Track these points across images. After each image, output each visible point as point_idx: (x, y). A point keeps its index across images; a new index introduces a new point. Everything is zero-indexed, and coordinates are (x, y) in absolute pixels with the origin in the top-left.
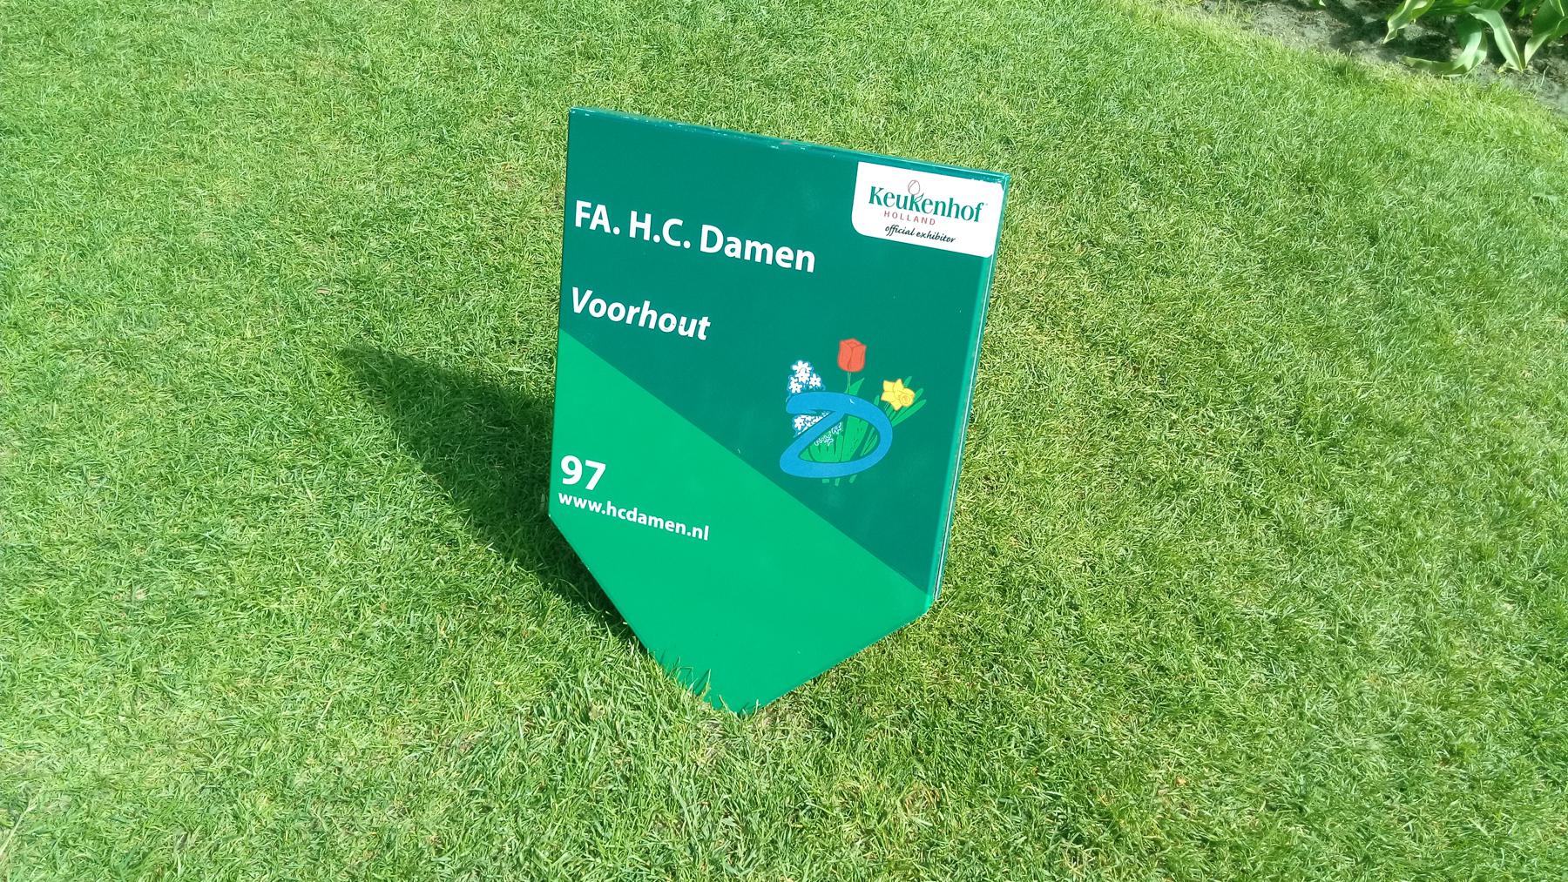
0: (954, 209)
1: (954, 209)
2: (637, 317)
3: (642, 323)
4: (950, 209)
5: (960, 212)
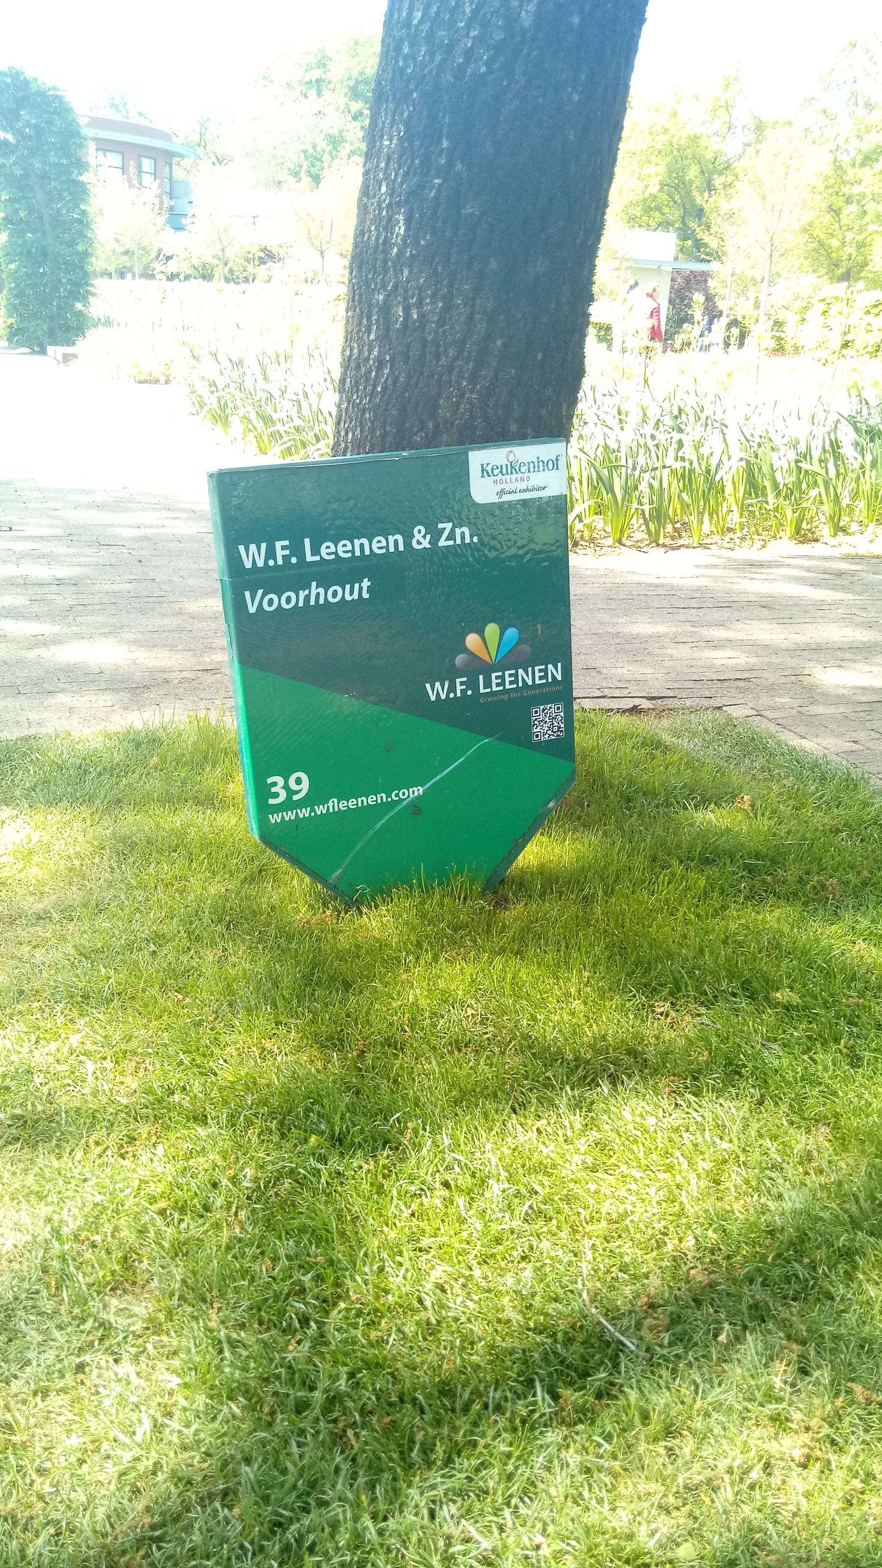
2: (307, 598)
3: (312, 603)
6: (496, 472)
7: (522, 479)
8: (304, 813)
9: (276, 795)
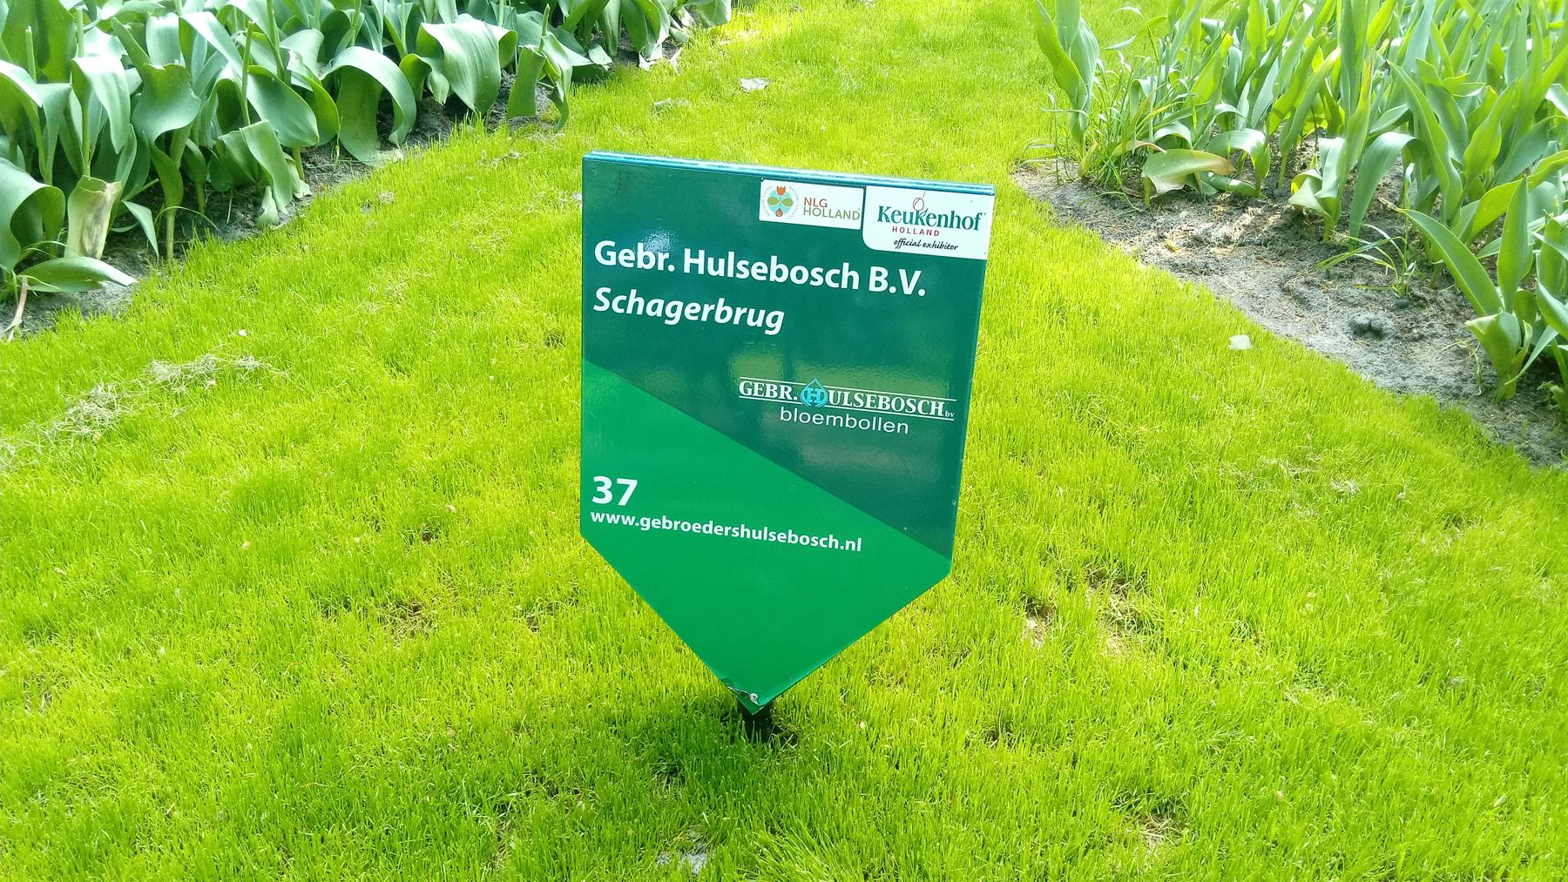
4: (952, 221)
6: (897, 218)
7: (929, 232)
8: (629, 521)
9: (602, 495)
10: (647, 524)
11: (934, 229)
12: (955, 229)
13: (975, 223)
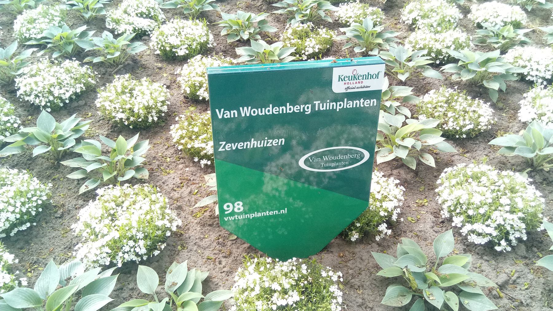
0: (370, 76)
1: (370, 76)
4: (369, 76)
5: (372, 77)
6: (346, 79)
7: (359, 82)
10: (252, 216)
11: (362, 80)
12: (369, 80)
13: (377, 76)
